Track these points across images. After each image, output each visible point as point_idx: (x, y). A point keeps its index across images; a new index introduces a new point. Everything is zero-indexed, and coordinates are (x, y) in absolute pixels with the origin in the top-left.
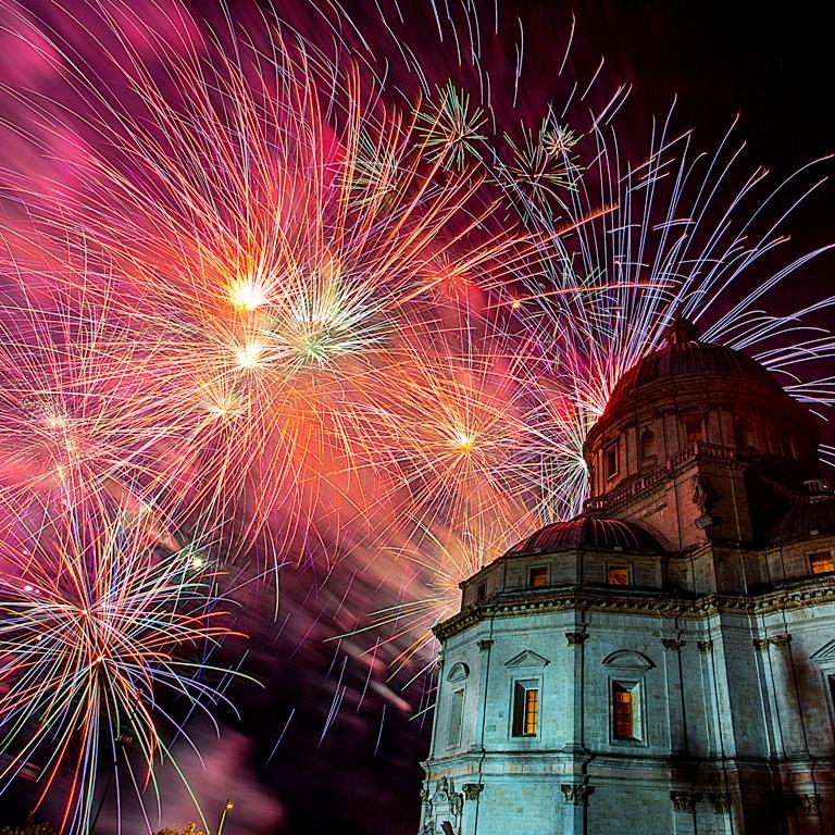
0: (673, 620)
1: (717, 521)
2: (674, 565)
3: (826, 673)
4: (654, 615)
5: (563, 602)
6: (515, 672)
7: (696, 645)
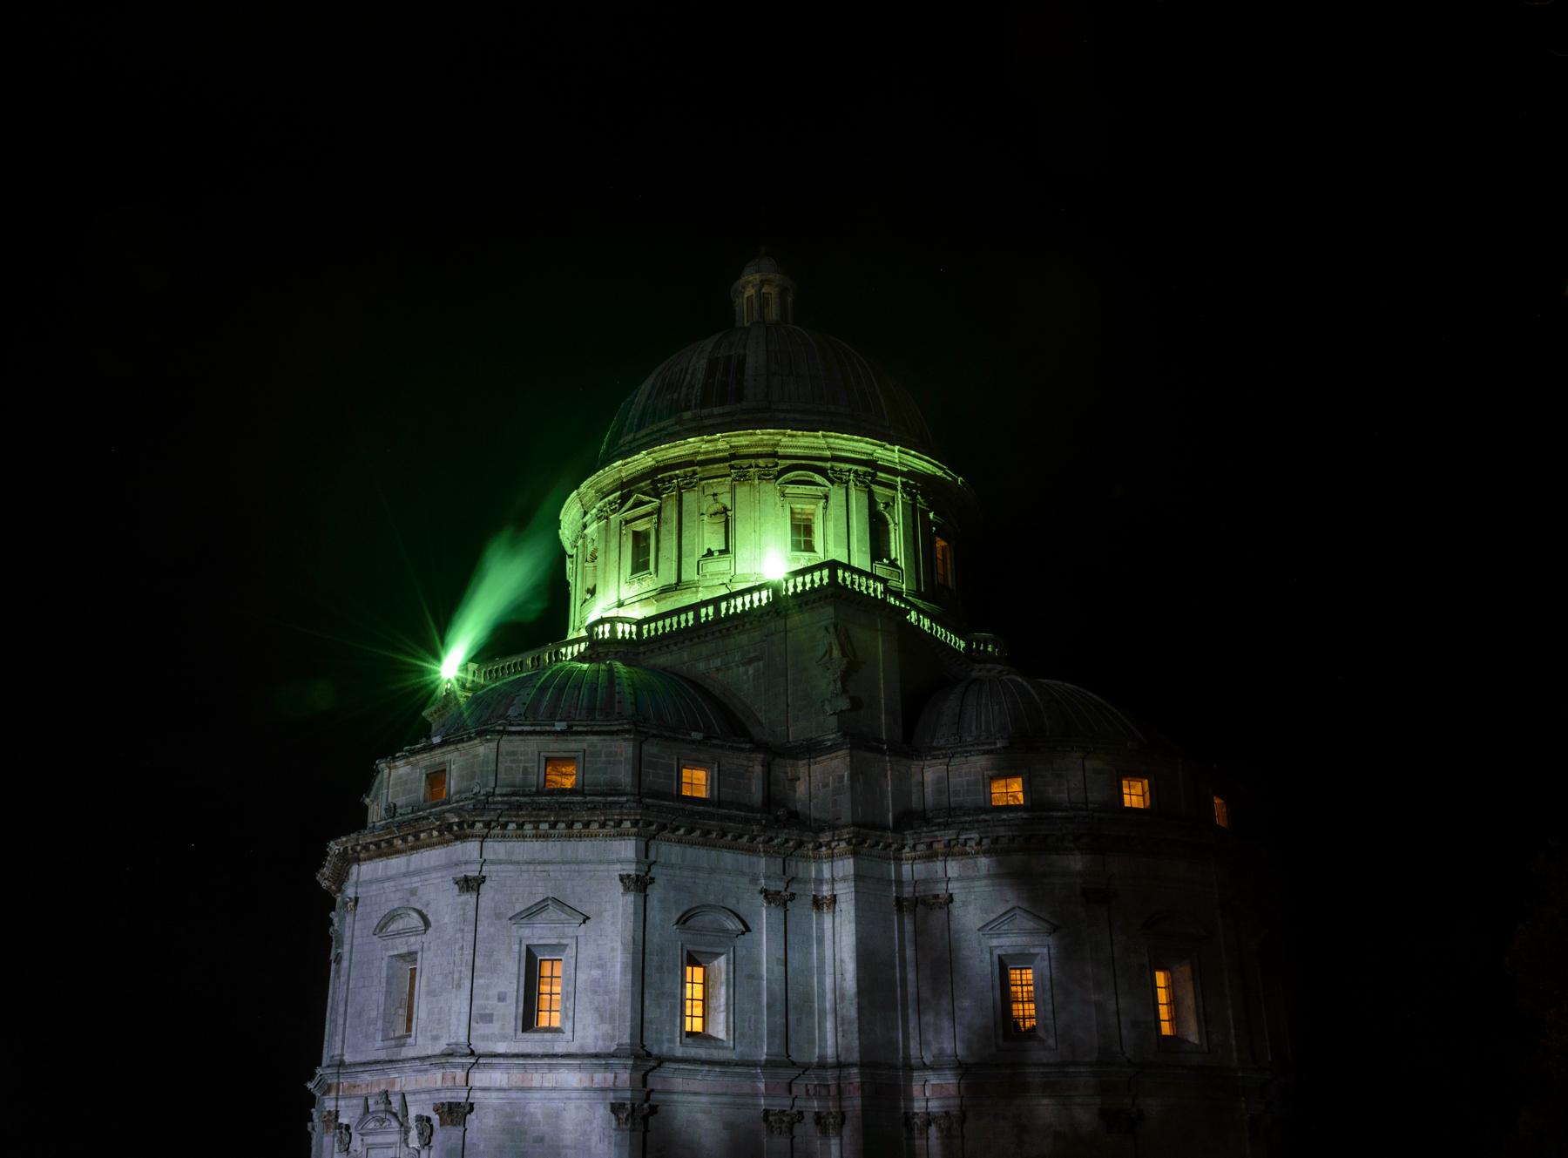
0: (780, 860)
1: (856, 704)
3: (997, 952)
4: (752, 851)
6: (526, 932)
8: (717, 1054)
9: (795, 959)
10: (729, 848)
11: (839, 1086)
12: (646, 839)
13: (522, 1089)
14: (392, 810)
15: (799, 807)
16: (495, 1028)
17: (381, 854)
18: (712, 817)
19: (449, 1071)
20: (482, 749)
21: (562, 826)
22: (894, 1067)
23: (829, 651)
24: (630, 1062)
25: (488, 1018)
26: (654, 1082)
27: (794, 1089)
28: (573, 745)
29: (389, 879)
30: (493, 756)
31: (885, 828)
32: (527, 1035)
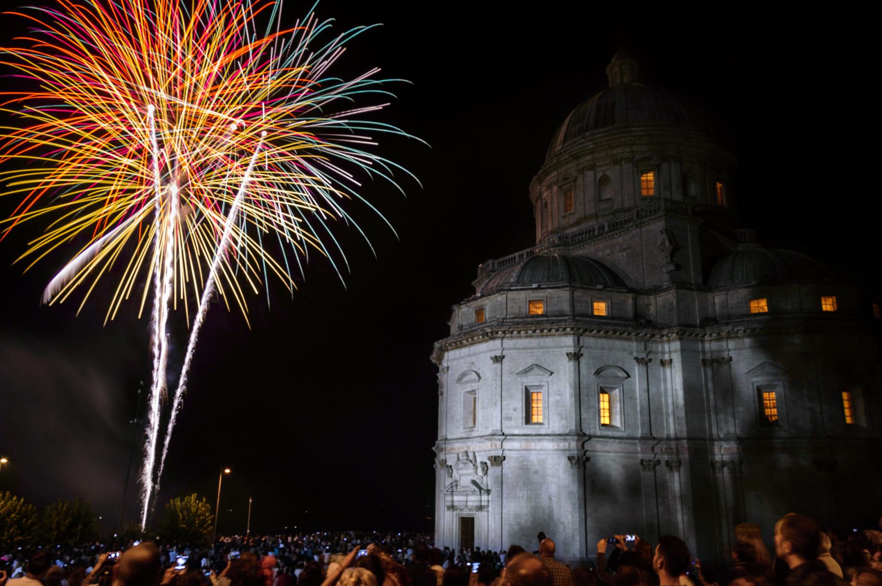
0: (643, 344)
1: (678, 267)
2: (643, 300)
3: (756, 385)
4: (629, 339)
5: (565, 329)
7: (659, 362)
8: (616, 434)
9: (653, 390)
10: (618, 338)
11: (677, 448)
12: (578, 337)
13: (527, 450)
14: (461, 327)
15: (652, 318)
16: (513, 423)
17: (457, 347)
18: (609, 324)
19: (494, 442)
20: (500, 298)
21: (538, 331)
22: (704, 439)
23: (663, 243)
24: (576, 438)
25: (509, 419)
26: (587, 446)
27: (656, 450)
28: (541, 294)
29: (462, 358)
30: (504, 301)
31: (695, 326)
32: (528, 426)
